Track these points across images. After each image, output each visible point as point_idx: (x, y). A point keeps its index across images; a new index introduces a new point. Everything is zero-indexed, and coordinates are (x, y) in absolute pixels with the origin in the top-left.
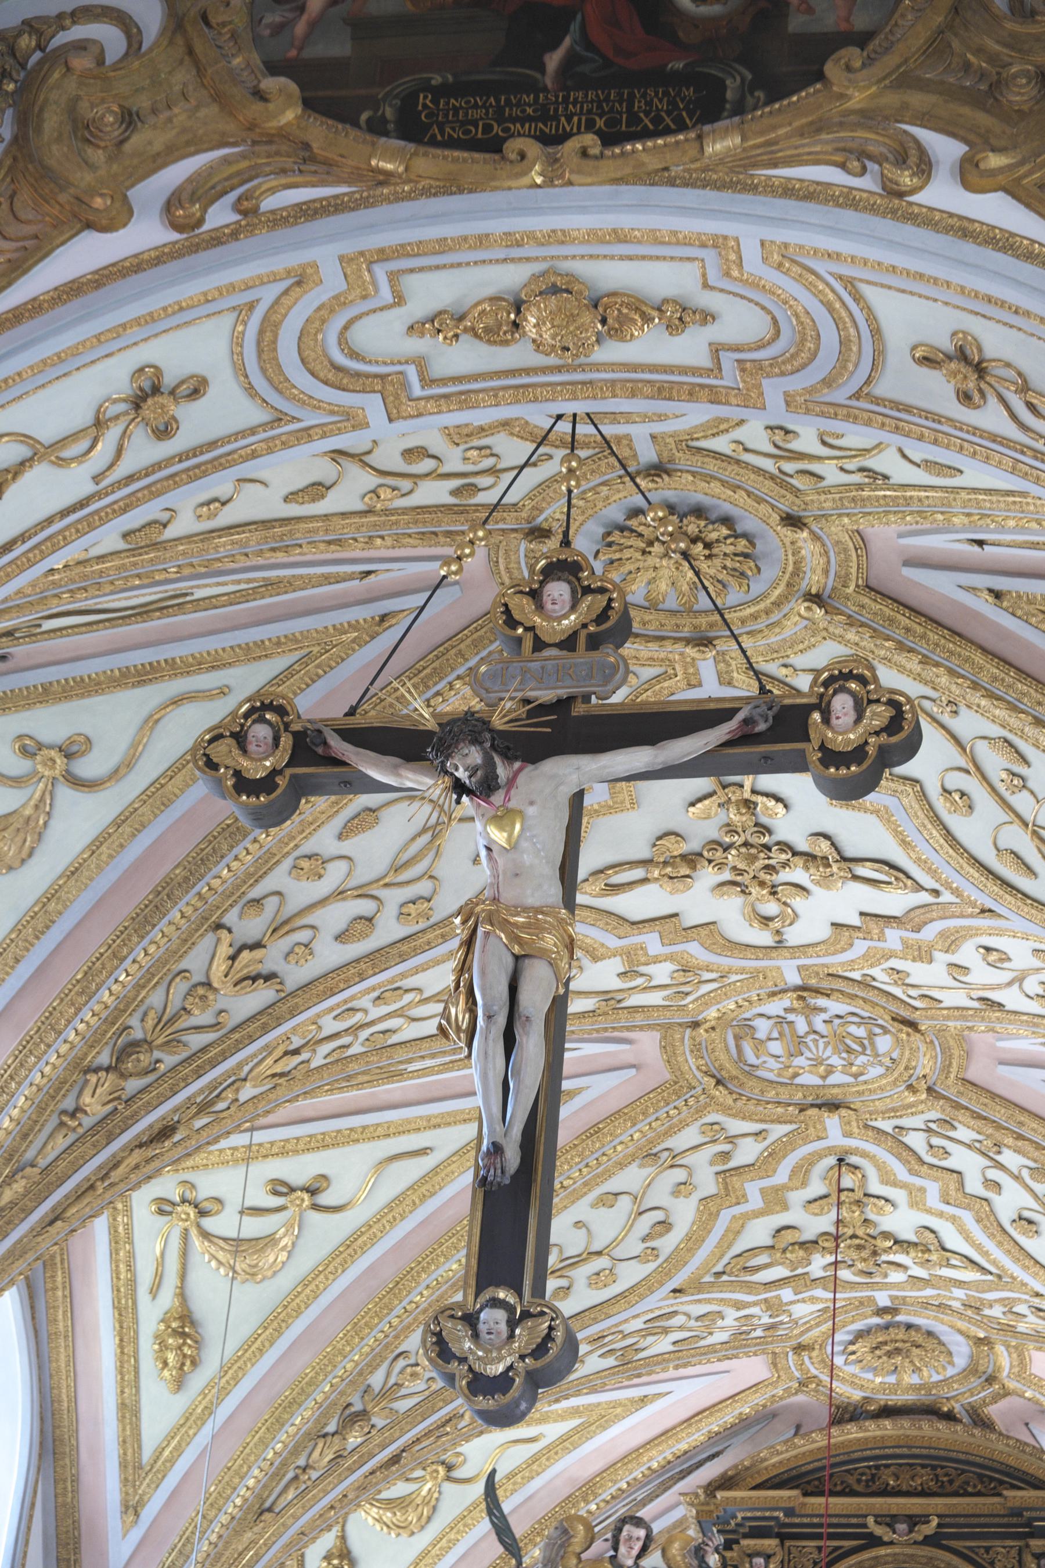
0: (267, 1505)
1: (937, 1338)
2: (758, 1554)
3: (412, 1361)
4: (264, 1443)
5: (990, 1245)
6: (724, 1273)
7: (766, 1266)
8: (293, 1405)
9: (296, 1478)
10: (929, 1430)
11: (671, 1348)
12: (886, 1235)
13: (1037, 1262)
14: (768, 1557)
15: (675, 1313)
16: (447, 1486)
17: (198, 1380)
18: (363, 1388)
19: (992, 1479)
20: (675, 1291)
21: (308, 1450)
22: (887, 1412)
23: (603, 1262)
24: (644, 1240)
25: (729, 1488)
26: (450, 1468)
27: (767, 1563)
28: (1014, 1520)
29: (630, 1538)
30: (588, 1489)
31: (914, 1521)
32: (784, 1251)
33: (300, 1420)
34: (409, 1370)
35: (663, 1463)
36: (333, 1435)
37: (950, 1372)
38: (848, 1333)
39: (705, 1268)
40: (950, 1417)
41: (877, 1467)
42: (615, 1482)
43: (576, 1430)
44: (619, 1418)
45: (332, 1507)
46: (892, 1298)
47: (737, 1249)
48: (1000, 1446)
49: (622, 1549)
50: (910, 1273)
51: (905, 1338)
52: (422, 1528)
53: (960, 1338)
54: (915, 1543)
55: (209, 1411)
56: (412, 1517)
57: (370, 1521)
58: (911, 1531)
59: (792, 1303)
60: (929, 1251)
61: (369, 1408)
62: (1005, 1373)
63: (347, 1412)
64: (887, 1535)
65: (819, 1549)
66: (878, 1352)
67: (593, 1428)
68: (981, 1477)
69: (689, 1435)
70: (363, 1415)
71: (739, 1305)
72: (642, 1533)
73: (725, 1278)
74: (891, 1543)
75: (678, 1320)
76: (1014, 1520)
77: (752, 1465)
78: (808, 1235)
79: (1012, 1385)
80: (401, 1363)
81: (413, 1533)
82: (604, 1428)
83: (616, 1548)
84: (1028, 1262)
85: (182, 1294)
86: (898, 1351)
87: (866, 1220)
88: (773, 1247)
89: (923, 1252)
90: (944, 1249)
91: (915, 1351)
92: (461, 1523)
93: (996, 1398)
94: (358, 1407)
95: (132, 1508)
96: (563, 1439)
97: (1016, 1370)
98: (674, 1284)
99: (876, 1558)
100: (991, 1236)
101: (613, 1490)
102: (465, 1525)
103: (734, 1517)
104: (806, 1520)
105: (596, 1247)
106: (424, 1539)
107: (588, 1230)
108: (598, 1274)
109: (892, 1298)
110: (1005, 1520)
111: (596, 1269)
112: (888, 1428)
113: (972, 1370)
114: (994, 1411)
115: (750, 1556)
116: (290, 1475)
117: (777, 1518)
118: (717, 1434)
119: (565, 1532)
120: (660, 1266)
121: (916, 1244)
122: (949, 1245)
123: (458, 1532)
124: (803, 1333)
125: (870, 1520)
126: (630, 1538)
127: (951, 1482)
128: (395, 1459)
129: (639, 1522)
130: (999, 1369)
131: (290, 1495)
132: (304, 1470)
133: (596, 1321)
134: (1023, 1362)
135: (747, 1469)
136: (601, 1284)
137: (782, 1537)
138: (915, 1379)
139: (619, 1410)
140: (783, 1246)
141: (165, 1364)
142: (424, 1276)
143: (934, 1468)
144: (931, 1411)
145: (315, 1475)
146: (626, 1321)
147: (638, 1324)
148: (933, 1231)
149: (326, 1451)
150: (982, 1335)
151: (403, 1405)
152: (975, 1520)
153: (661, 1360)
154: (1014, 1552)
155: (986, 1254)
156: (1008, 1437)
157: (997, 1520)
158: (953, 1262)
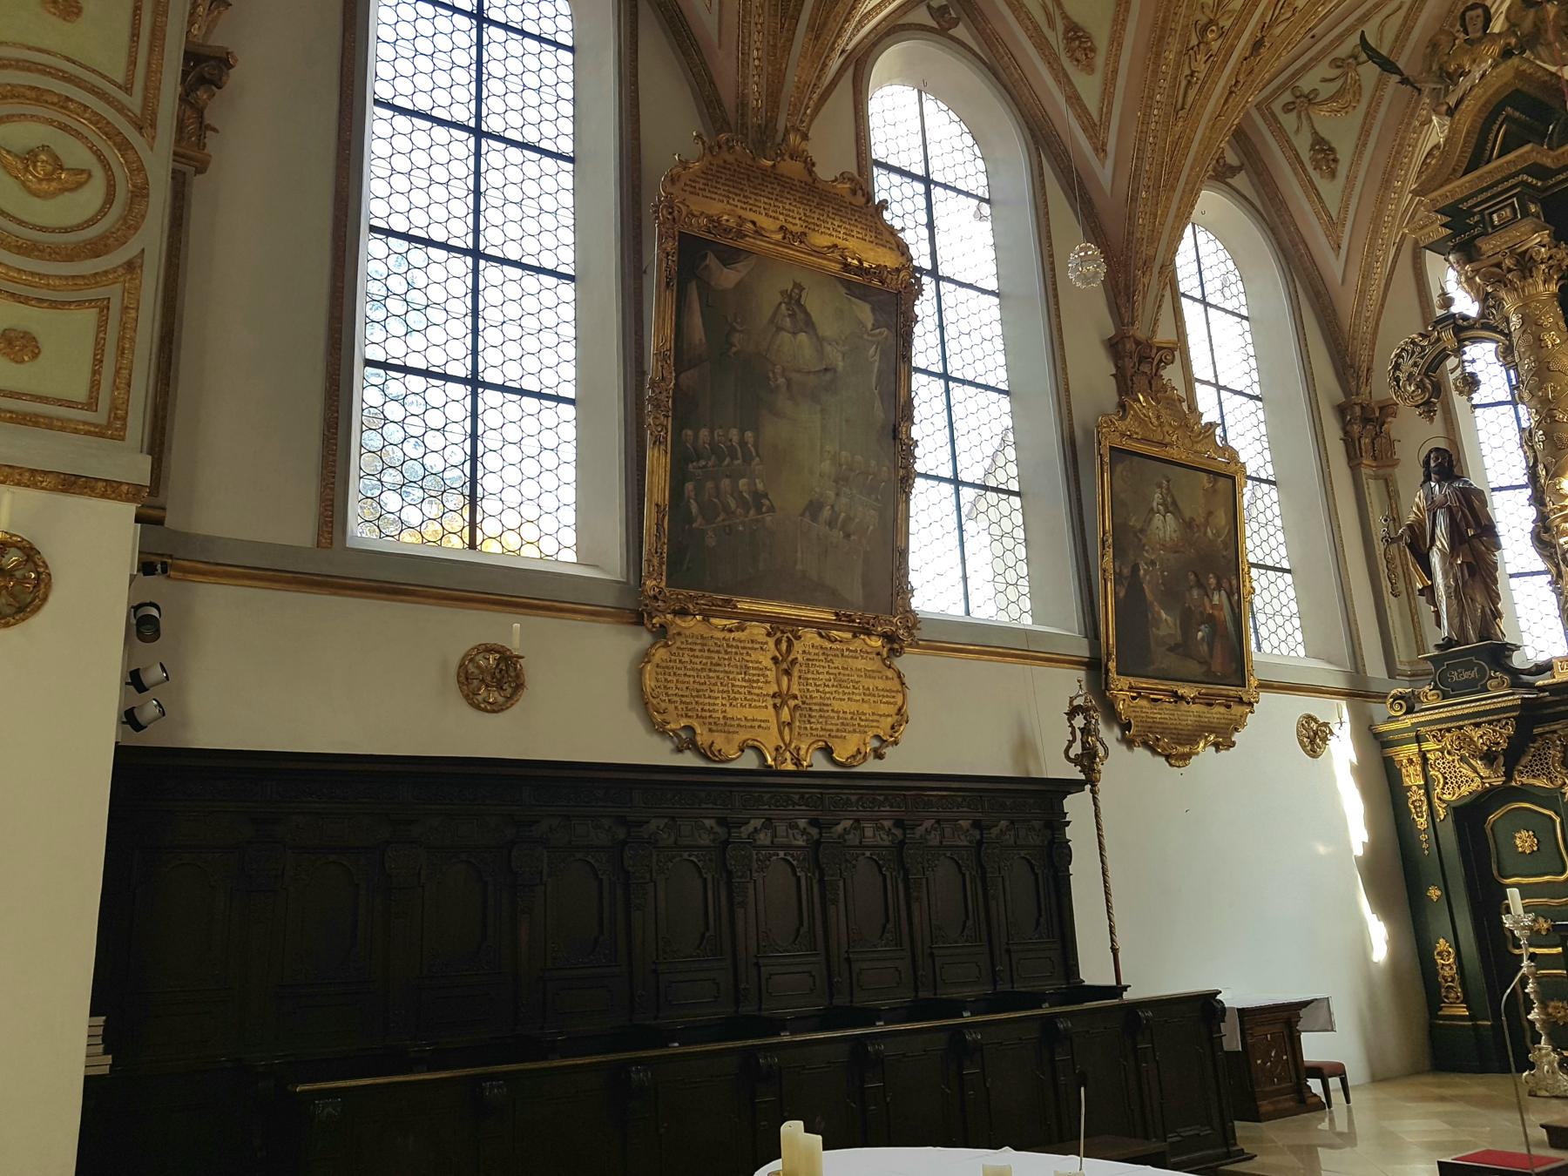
9: (1189, 82)
17: (1100, 60)
18: (1199, 6)
21: (1187, 63)
36: (1198, 45)
55: (1115, 71)
57: (1327, 114)
63: (1199, 27)
72: (1480, 11)
85: (1065, 17)
94: (1204, 20)
95: (1100, 149)
116: (1184, 83)
126: (1471, 19)
128: (1257, 45)
131: (1192, 93)
132: (1192, 76)
141: (1078, 60)
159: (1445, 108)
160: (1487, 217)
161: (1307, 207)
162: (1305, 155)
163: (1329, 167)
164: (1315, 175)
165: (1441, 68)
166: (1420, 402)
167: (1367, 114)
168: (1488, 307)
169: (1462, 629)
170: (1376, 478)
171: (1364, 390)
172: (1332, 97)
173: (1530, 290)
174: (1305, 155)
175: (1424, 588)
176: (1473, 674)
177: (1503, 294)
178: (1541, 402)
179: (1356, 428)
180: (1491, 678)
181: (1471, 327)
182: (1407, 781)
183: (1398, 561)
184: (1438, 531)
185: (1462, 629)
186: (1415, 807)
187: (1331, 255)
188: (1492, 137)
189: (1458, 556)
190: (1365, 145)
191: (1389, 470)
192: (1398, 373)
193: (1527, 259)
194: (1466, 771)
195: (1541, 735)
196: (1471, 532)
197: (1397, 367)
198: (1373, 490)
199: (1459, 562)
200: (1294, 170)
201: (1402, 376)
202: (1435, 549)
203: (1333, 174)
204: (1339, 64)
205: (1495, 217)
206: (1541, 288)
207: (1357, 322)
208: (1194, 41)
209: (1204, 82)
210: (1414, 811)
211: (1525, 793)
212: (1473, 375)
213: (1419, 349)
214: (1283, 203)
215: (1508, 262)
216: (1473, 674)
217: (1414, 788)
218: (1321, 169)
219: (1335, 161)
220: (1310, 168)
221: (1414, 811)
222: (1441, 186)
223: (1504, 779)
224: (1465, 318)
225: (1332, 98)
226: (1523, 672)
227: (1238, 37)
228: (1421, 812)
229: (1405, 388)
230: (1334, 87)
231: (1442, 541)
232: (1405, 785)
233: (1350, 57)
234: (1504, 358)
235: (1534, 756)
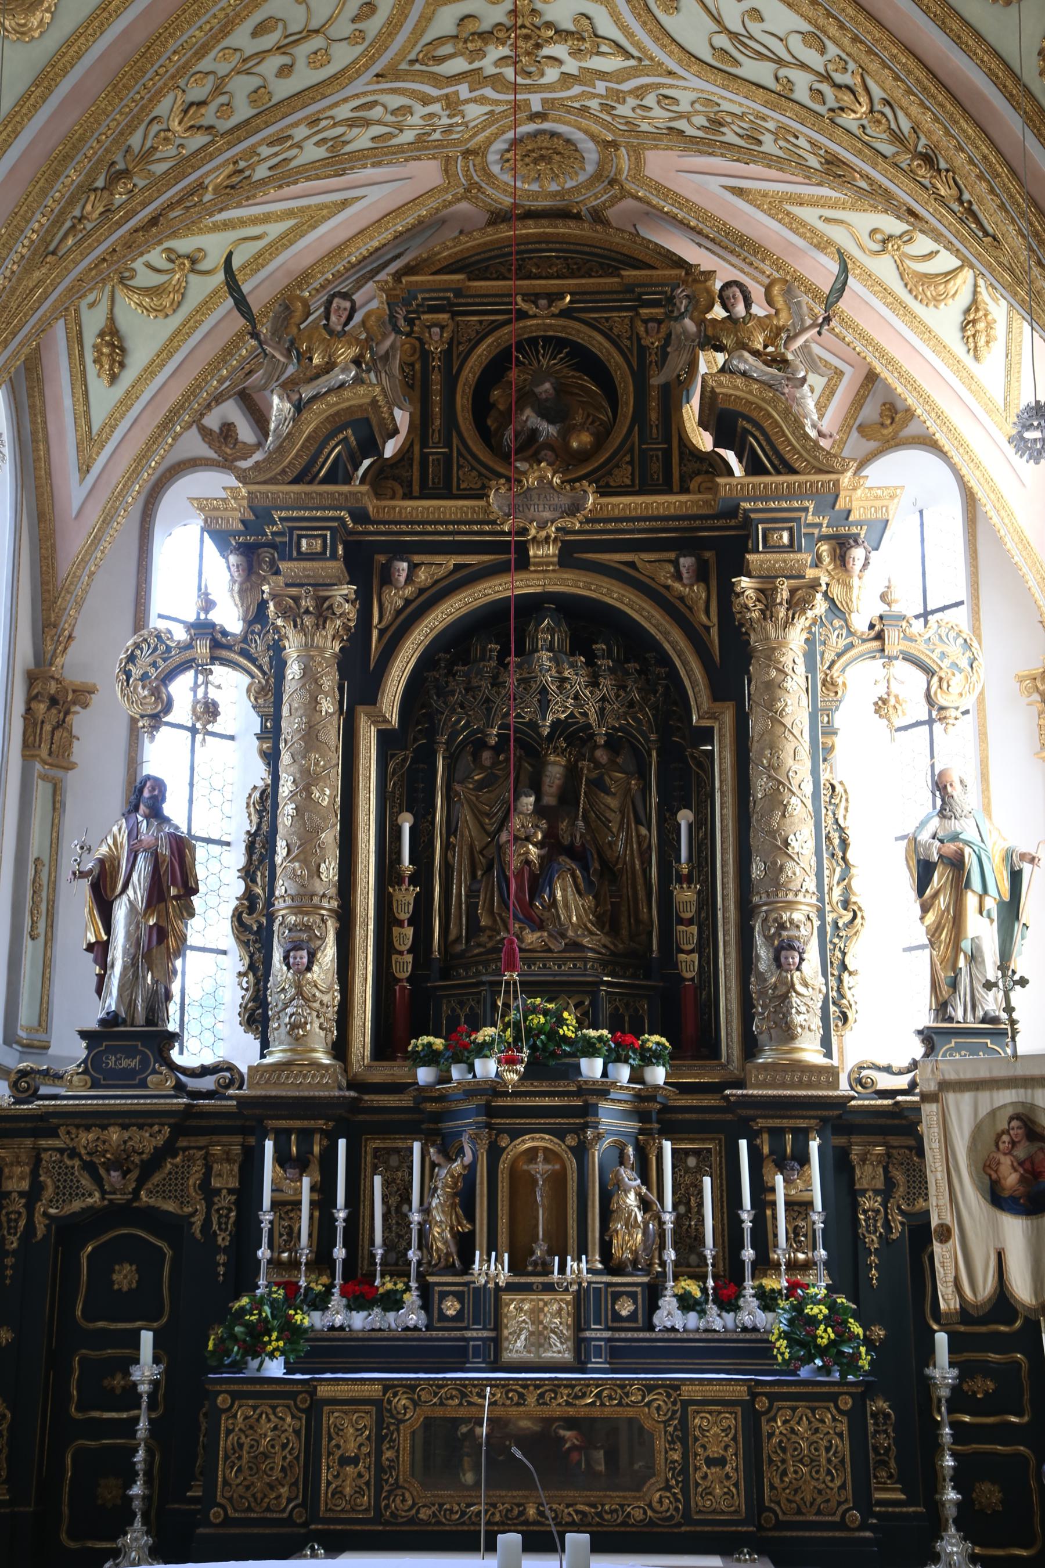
0: (51, 248)
1: (574, 145)
2: (435, 325)
3: (164, 127)
4: (44, 193)
5: (635, 26)
6: (417, 61)
7: (451, 56)
8: (66, 158)
9: (73, 226)
10: (563, 229)
11: (371, 145)
12: (549, 25)
13: (674, 40)
14: (442, 328)
15: (374, 104)
16: (193, 278)
18: (124, 148)
19: (609, 266)
20: (377, 76)
21: (82, 202)
22: (531, 215)
23: (317, 42)
24: (353, 21)
25: (413, 274)
26: (194, 261)
27: (442, 332)
28: (628, 296)
29: (339, 308)
30: (304, 277)
31: (554, 297)
32: (465, 42)
33: (73, 176)
34: (162, 134)
35: (360, 257)
36: (102, 190)
37: (582, 178)
38: (505, 141)
39: (402, 54)
40: (577, 217)
41: (523, 260)
42: (323, 274)
43: (292, 230)
44: (326, 219)
45: (104, 260)
46: (544, 101)
47: (428, 38)
48: (617, 240)
49: (333, 318)
50: (564, 69)
51: (549, 145)
52: (174, 311)
53: (591, 145)
54: (554, 316)
56: (166, 302)
57: (133, 305)
58: (550, 306)
59: (467, 101)
60: (583, 39)
61: (130, 167)
62: (624, 176)
63: (113, 170)
64: (532, 310)
65: (481, 322)
66: (527, 160)
67: (305, 227)
68: (601, 264)
69: (380, 234)
70: (126, 173)
71: (426, 101)
73: (417, 67)
74: (535, 316)
75: (377, 112)
76: (628, 296)
77: (429, 258)
78: (486, 26)
79: (630, 186)
80: (155, 128)
81: (167, 316)
82: (315, 227)
83: (328, 318)
84: (667, 41)
86: (542, 157)
87: (533, 10)
88: (456, 37)
89: (578, 40)
90: (597, 36)
91: (557, 158)
92: (206, 306)
93: (615, 200)
94: (121, 166)
96: (281, 237)
97: (632, 173)
98: (376, 68)
99: (525, 327)
100: (638, 16)
101: (321, 281)
102: (209, 309)
103: (416, 299)
104: (469, 300)
105: (314, 24)
106: (175, 321)
107: (308, 7)
108: (315, 53)
109: (544, 101)
110: (621, 296)
111: (314, 49)
112: (531, 229)
113: (598, 176)
114: (611, 214)
115: (429, 327)
116: (68, 224)
117: (448, 299)
118: (401, 234)
119: (287, 308)
120: (366, 50)
121: (572, 33)
122: (600, 32)
123: (203, 314)
124: (472, 137)
125: (519, 299)
126: (339, 308)
127: (579, 269)
128: (154, 221)
129: (346, 296)
130: (619, 172)
131: (70, 242)
132: (80, 220)
133: (314, 101)
134: (638, 163)
135: (425, 260)
136: (318, 64)
137: (454, 314)
138: (554, 187)
139: (325, 212)
140: (465, 35)
142: (171, 41)
143: (566, 258)
144: (564, 214)
145: (89, 226)
146: (336, 104)
147: (344, 112)
148: (588, 18)
149: (97, 204)
150: (610, 139)
151: (160, 168)
152: (599, 297)
153: (360, 158)
154: (627, 321)
155: (629, 35)
156: (623, 231)
157: (615, 296)
158: (604, 49)
159: (296, 397)
160: (295, 537)
161: (67, 402)
162: (90, 338)
163: (111, 369)
164: (92, 369)
165: (292, 342)
166: (149, 712)
167: (178, 332)
168: (253, 632)
169: (131, 1006)
170: (44, 778)
171: (59, 661)
172: (147, 289)
173: (318, 640)
174: (90, 338)
175: (97, 942)
176: (134, 1063)
177: (290, 631)
178: (301, 772)
179: (41, 707)
180: (155, 1072)
181: (229, 647)
182: (11, 1185)
183: (44, 895)
184: (135, 876)
185: (131, 1006)
186: (9, 1221)
187: (74, 475)
188: (326, 451)
189: (152, 914)
190: (162, 366)
191: (59, 773)
192: (131, 666)
193: (325, 605)
194: (86, 1182)
195: (185, 1149)
196: (173, 891)
197: (131, 658)
198: (41, 791)
199: (151, 923)
200: (70, 349)
201: (136, 672)
202: (124, 898)
203: (113, 378)
204: (173, 257)
205: (304, 542)
206: (329, 644)
207: (78, 573)
208: (100, 183)
209: (89, 235)
210: (5, 1225)
211: (152, 1219)
212: (215, 704)
213: (163, 648)
214: (40, 380)
215: (307, 603)
216: (134, 1063)
217: (15, 1195)
218: (102, 366)
219: (122, 365)
220: (89, 356)
221: (5, 1225)
222: (265, 482)
223: (130, 1196)
224: (225, 633)
225: (149, 291)
226: (184, 1071)
227: (144, 205)
228: (16, 1228)
229: (135, 688)
230: (156, 279)
231: (136, 892)
232: (4, 1189)
233: (188, 257)
234: (256, 699)
235: (170, 1173)
